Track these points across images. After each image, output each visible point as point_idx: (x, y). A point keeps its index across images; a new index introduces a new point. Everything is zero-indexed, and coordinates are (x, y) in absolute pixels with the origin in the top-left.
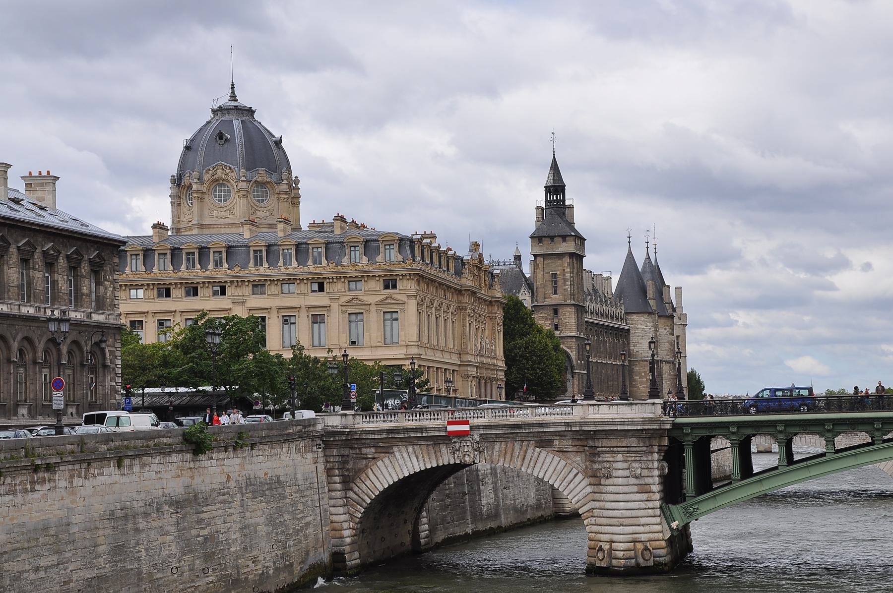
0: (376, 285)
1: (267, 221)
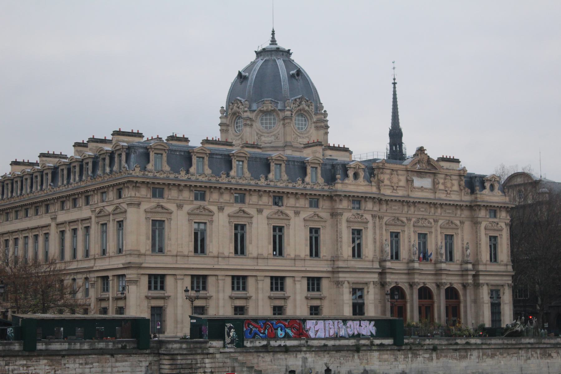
0: (111, 195)
1: (271, 145)
